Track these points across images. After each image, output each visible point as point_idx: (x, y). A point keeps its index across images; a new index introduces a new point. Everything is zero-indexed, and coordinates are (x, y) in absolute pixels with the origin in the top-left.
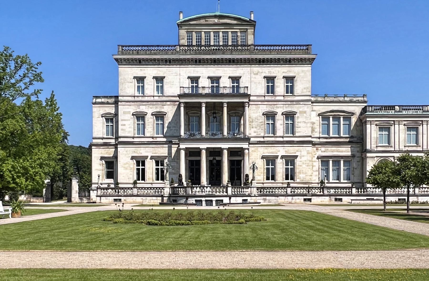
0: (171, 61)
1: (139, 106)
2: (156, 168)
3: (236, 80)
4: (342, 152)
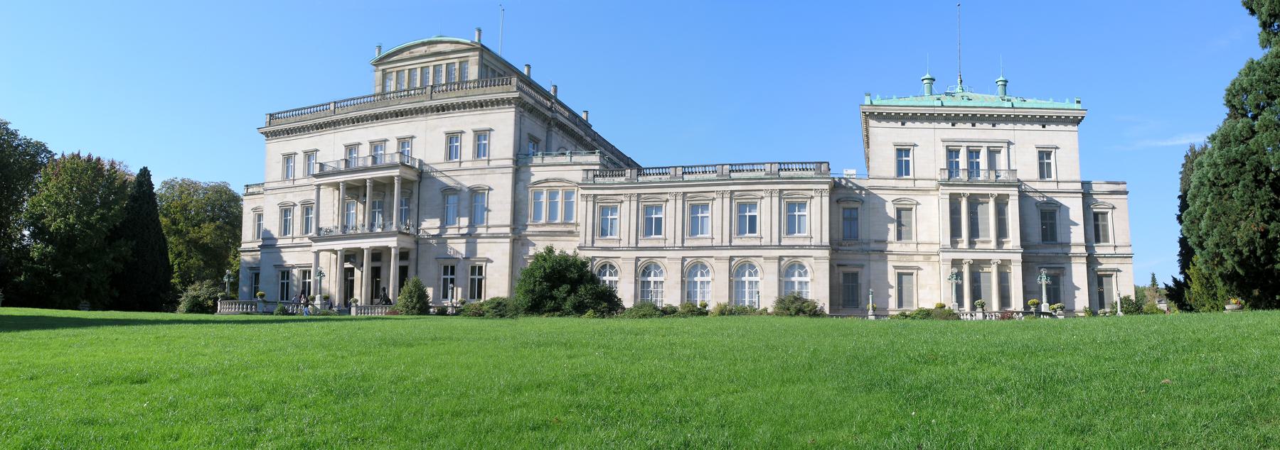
3: (404, 142)
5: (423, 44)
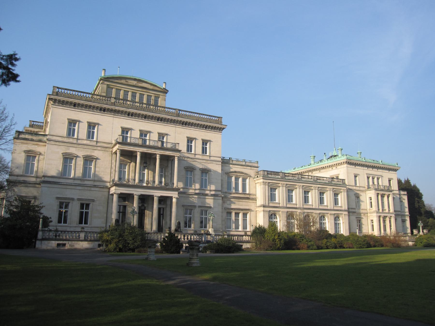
0: (106, 110)
1: (69, 147)
2: (80, 211)
4: (242, 205)
5: (135, 80)
